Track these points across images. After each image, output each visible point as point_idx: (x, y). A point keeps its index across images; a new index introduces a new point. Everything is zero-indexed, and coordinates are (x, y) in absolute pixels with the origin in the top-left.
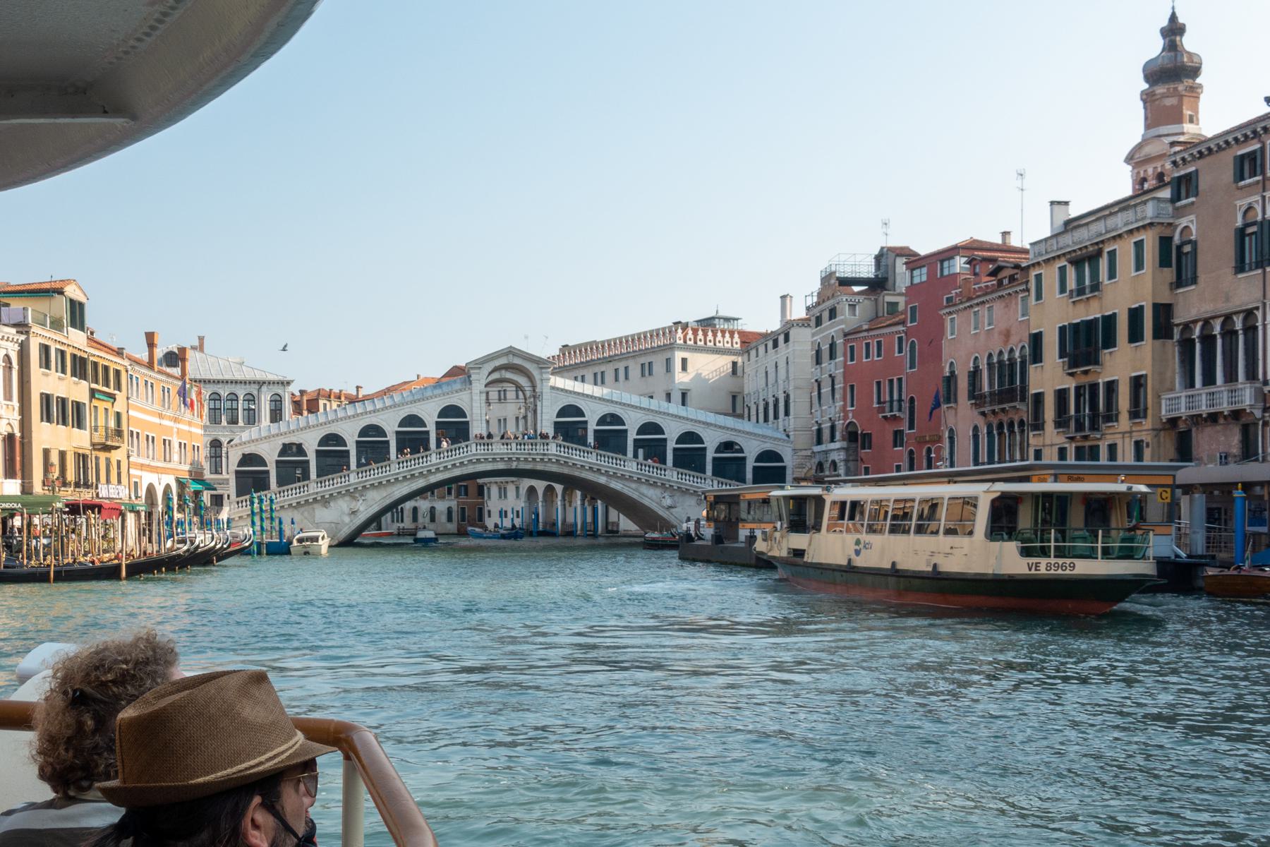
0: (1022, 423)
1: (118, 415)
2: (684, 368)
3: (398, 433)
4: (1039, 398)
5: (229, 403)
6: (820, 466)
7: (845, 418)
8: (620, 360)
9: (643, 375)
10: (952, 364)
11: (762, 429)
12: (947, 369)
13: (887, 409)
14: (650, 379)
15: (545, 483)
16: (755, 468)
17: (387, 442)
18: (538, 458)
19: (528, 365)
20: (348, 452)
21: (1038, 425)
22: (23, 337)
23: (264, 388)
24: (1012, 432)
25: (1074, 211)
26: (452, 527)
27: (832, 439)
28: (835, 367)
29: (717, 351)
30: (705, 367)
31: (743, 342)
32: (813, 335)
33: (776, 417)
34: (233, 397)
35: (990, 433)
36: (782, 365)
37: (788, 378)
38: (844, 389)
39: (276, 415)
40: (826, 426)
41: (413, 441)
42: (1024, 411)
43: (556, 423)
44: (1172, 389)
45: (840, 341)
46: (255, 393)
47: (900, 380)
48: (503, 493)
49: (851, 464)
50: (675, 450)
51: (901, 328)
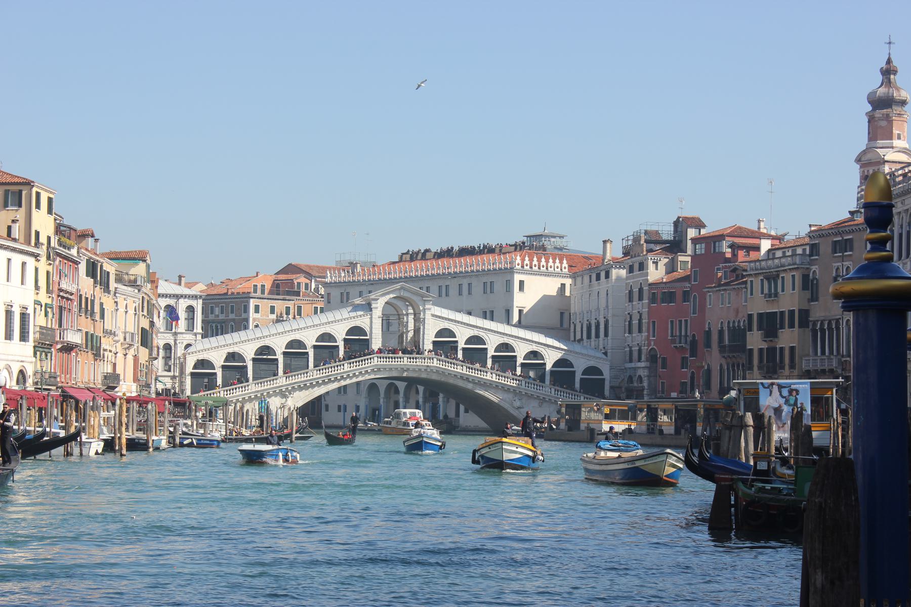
2: (521, 288)
3: (315, 347)
4: (751, 350)
6: (630, 379)
7: (649, 345)
8: (464, 277)
13: (678, 341)
16: (581, 379)
29: (548, 274)
31: (570, 266)
35: (728, 369)
37: (607, 307)
38: (648, 323)
42: (743, 359)
43: (434, 343)
44: (808, 355)
45: (646, 288)
47: (686, 321)
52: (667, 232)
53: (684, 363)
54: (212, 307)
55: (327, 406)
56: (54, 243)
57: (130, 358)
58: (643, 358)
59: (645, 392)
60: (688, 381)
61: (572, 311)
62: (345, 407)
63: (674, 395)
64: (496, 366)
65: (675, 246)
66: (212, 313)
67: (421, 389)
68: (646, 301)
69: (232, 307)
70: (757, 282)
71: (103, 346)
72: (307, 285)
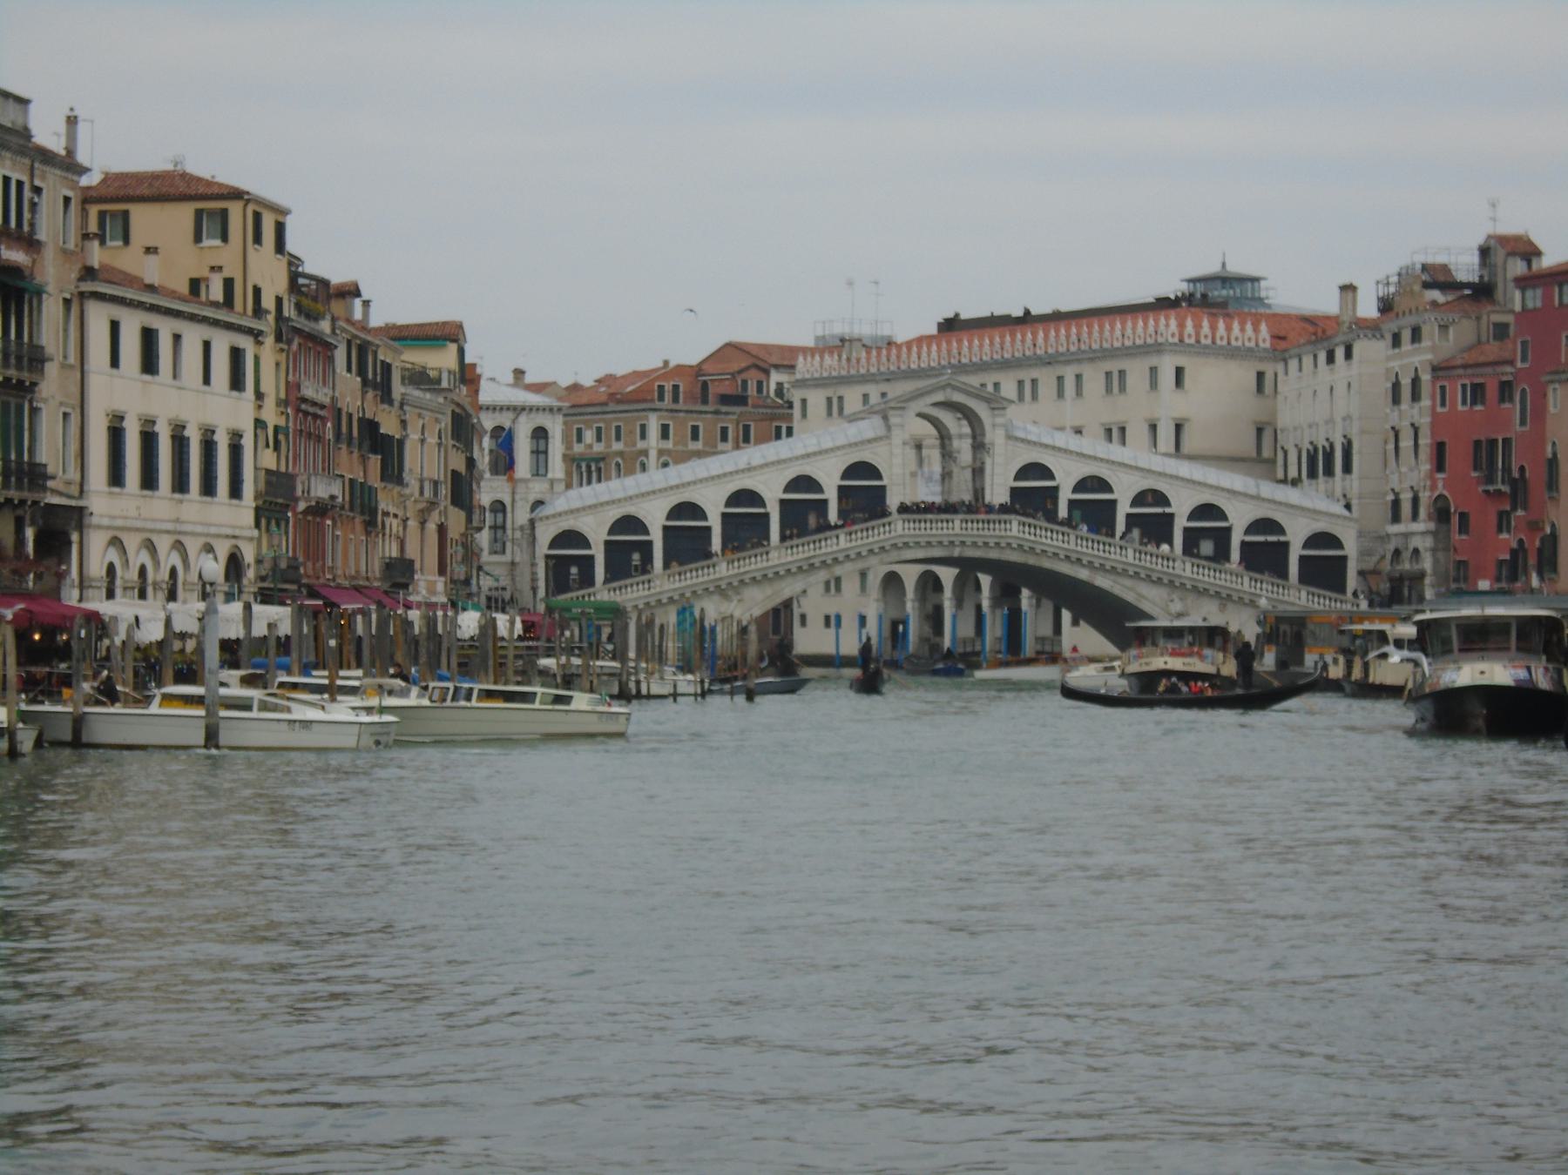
7: (1433, 487)
8: (1068, 362)
9: (1109, 390)
15: (922, 568)
16: (1302, 559)
17: (766, 516)
18: (992, 542)
20: (708, 529)
23: (523, 418)
27: (1415, 516)
28: (1419, 413)
32: (1389, 359)
36: (1340, 389)
40: (1406, 497)
41: (803, 514)
45: (1426, 377)
49: (1440, 555)
50: (1186, 530)
51: (1509, 369)
52: (1466, 267)
53: (1503, 521)
54: (579, 431)
55: (803, 618)
56: (289, 311)
57: (432, 527)
59: (1427, 581)
61: (1279, 426)
62: (838, 618)
63: (1484, 585)
64: (1136, 533)
65: (1482, 292)
66: (580, 440)
67: (985, 580)
69: (618, 429)
71: (382, 506)
72: (760, 384)
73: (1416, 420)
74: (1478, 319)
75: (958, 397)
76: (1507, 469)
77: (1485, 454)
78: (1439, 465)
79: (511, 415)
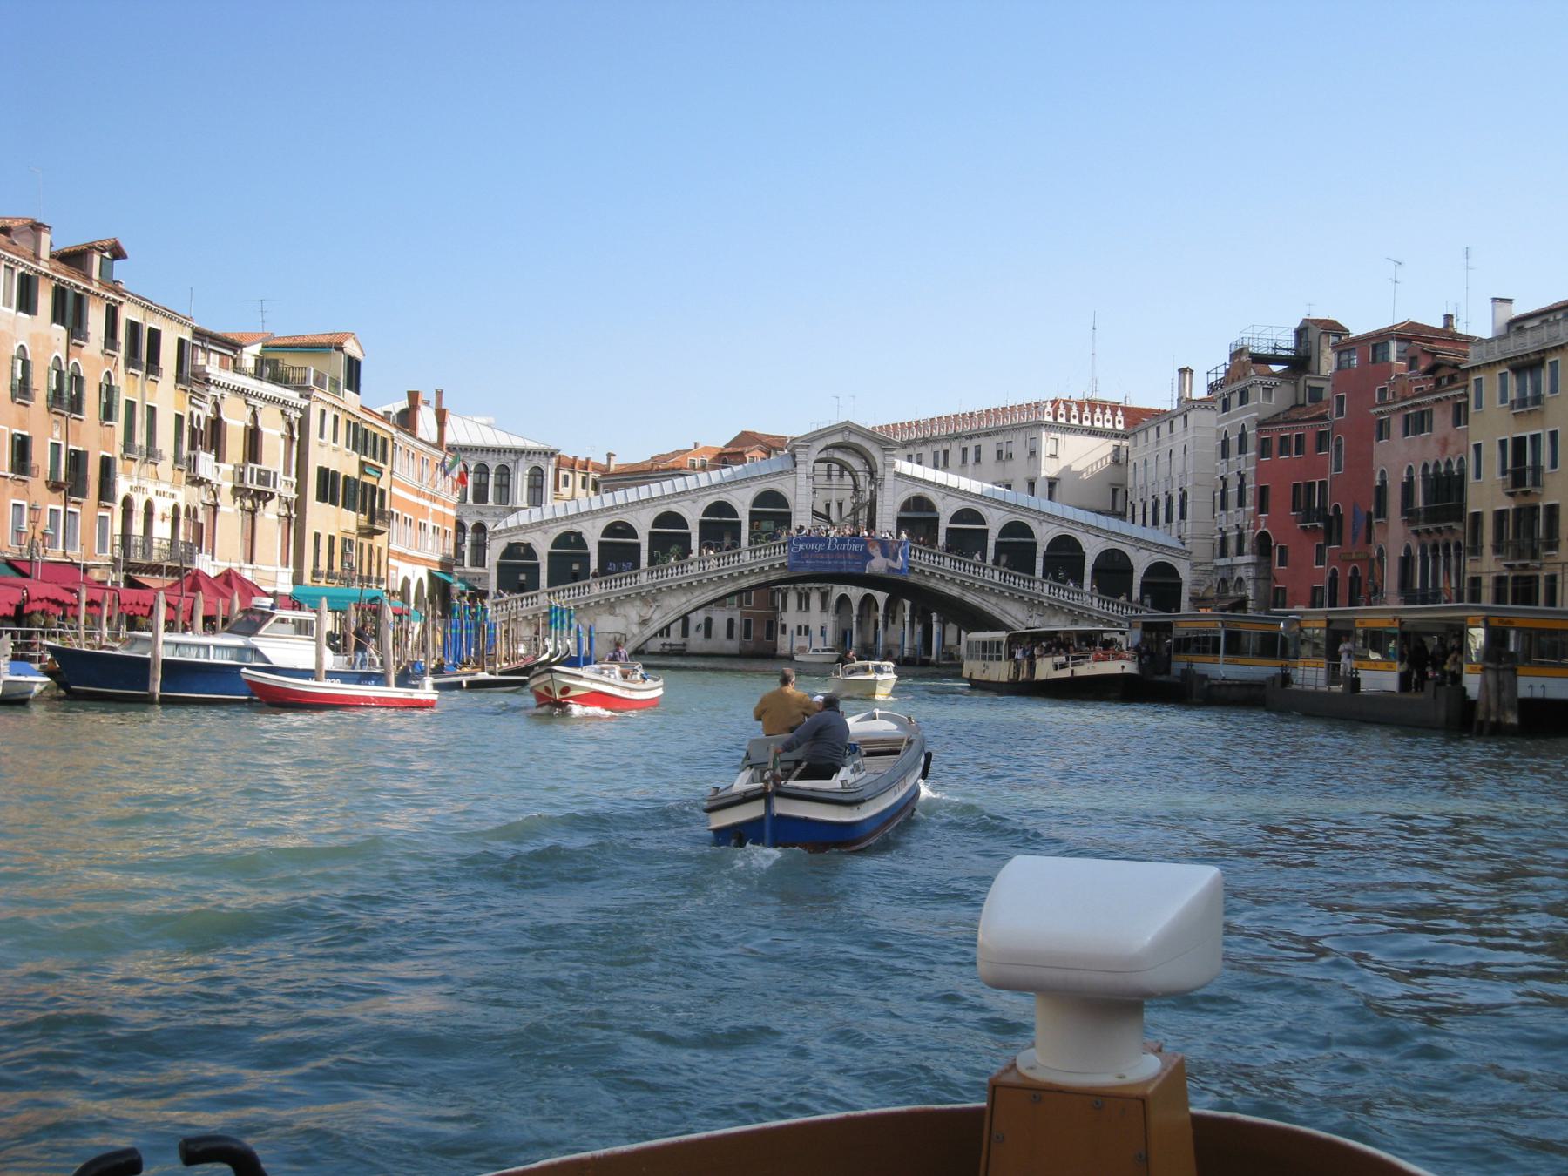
0: (1458, 546)
1: (382, 492)
4: (1477, 517)
5: (485, 476)
7: (1257, 526)
8: (970, 437)
10: (1383, 472)
11: (1149, 534)
12: (1378, 478)
14: (1009, 464)
17: (689, 535)
19: (867, 445)
20: (638, 545)
21: (1476, 549)
22: (304, 403)
23: (523, 460)
24: (1447, 556)
25: (1518, 310)
26: (733, 646)
29: (1093, 432)
30: (1078, 455)
32: (1219, 421)
33: (1169, 519)
34: (482, 470)
36: (1178, 452)
39: (536, 498)
45: (1251, 432)
46: (511, 465)
48: (804, 600)
55: (784, 627)
58: (1246, 547)
59: (1250, 605)
60: (1325, 584)
61: (1130, 484)
62: (807, 628)
64: (1003, 559)
65: (1299, 362)
68: (1252, 453)
70: (1491, 383)
73: (1243, 469)
74: (1296, 384)
75: (854, 439)
76: (1323, 508)
77: (1303, 497)
78: (1262, 506)
79: (513, 457)
